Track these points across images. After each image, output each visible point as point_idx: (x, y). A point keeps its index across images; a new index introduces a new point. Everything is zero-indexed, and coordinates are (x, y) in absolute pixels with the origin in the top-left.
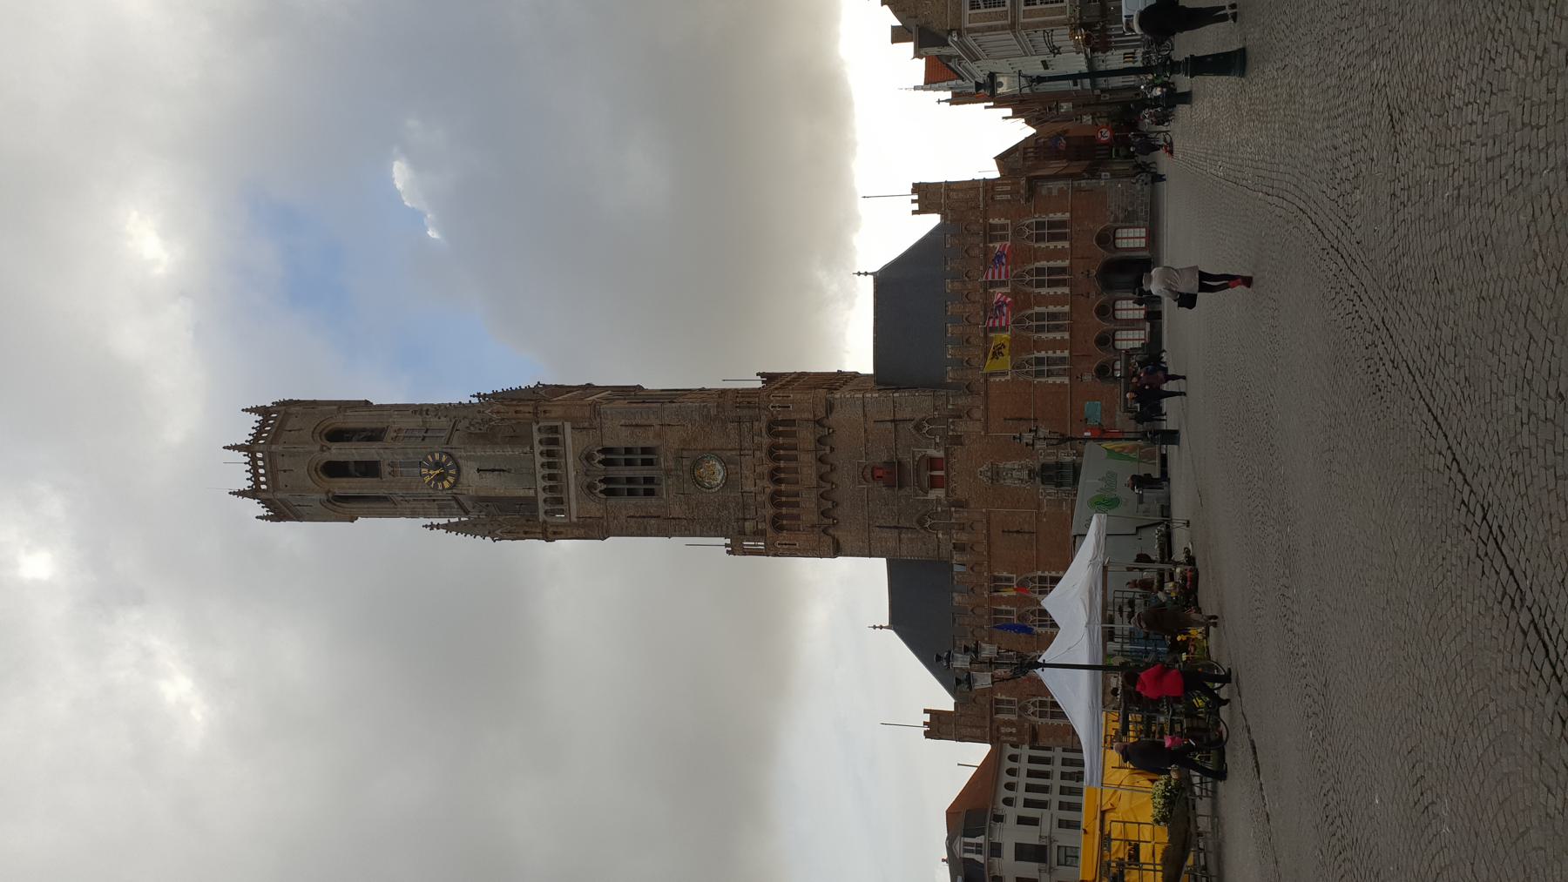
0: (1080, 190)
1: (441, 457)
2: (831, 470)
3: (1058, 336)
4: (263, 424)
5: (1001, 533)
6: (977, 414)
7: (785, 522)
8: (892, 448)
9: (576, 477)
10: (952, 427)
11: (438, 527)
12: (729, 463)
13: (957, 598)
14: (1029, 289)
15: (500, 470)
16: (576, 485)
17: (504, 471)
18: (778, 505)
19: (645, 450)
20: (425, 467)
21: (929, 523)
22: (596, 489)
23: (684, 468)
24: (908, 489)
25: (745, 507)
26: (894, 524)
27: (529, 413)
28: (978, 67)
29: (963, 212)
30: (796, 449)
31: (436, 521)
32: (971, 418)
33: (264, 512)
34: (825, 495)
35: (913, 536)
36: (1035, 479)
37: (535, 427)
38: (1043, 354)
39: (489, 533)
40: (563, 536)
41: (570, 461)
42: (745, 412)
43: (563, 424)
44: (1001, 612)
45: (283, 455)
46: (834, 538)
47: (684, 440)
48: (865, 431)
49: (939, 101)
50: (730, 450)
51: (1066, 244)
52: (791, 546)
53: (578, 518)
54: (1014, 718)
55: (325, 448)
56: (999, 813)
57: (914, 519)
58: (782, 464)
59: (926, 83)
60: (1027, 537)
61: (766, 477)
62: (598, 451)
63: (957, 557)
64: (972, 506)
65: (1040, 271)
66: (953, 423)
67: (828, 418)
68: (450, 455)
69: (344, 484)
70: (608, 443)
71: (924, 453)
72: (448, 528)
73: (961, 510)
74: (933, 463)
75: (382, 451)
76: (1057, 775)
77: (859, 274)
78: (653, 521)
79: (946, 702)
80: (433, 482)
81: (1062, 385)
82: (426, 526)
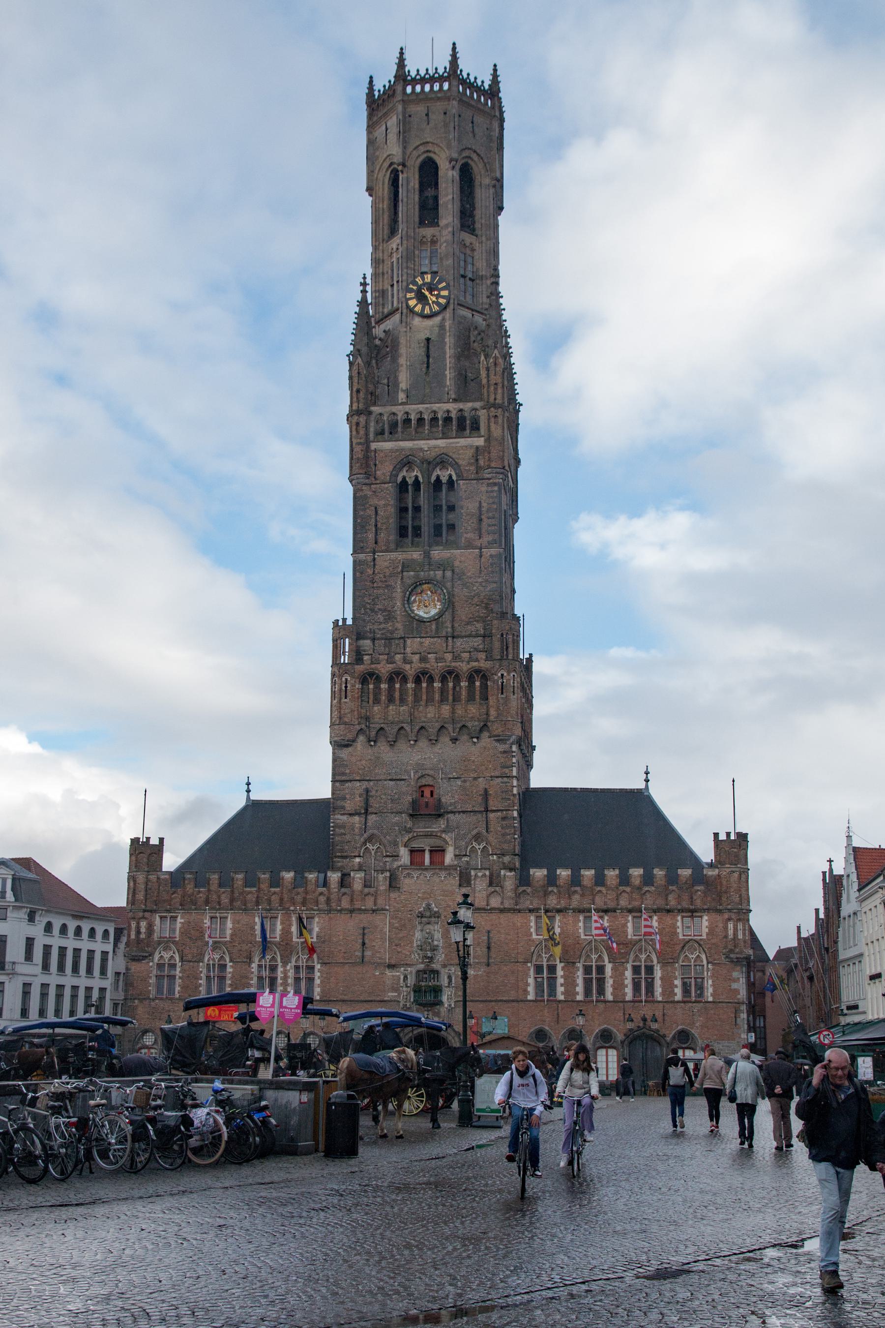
0: (737, 1012)
1: (443, 297)
2: (431, 740)
3: (580, 989)
4: (479, 89)
5: (362, 926)
6: (495, 902)
7: (371, 686)
9: (421, 449)
10: (480, 874)
11: (364, 292)
12: (437, 624)
13: (288, 876)
15: (428, 361)
16: (411, 449)
17: (428, 367)
18: (391, 680)
19: (452, 527)
20: (433, 279)
21: (371, 848)
22: (407, 471)
23: (432, 573)
27: (495, 399)
28: (871, 910)
29: (716, 888)
30: (454, 701)
31: (369, 288)
32: (490, 894)
33: (380, 85)
34: (402, 732)
35: (357, 830)
36: (422, 963)
37: (478, 405)
38: (560, 972)
39: (359, 350)
40: (354, 433)
41: (441, 443)
42: (497, 645)
43: (483, 436)
44: (274, 925)
45: (445, 113)
46: (354, 741)
47: (464, 574)
49: (830, 861)
50: (453, 627)
51: (679, 997)
52: (343, 693)
53: (375, 451)
54: (156, 936)
55: (453, 163)
56: (37, 918)
57: (375, 832)
58: (437, 685)
59: (855, 849)
60: (359, 954)
61: (423, 665)
63: (334, 877)
64: (392, 895)
65: (650, 969)
66: (484, 875)
67: (490, 737)
68: (445, 308)
69: (412, 184)
72: (363, 303)
74: (438, 852)
75: (450, 229)
76: (75, 981)
77: (647, 773)
78: (371, 536)
79: (171, 861)
80: (415, 288)
81: (526, 992)
82: (364, 278)
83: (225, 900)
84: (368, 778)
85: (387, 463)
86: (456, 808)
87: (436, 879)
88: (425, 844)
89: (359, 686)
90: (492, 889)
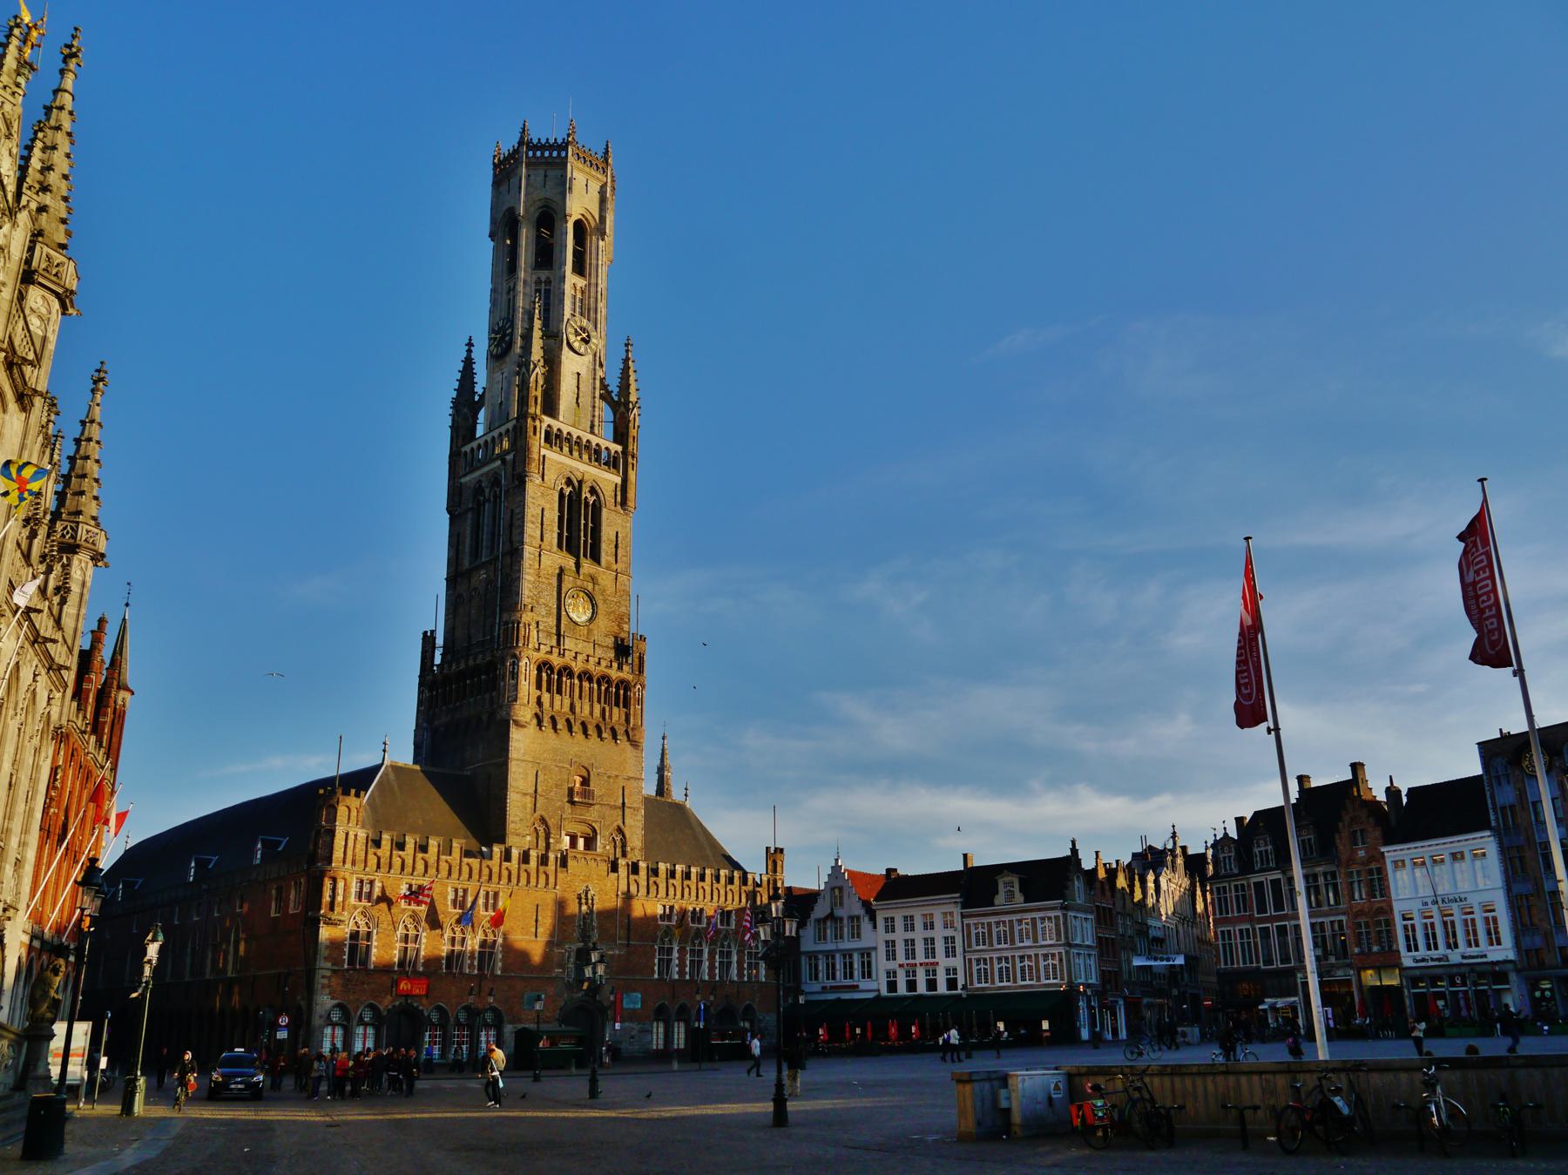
1: (594, 344)
3: (687, 969)
8: (602, 800)
14: (719, 944)
15: (578, 394)
16: (571, 467)
18: (560, 674)
24: (570, 811)
25: (549, 634)
26: (539, 790)
37: (619, 448)
48: (617, 776)
57: (544, 813)
62: (595, 500)
70: (604, 511)
71: (598, 832)
73: (559, 863)
77: (686, 789)
78: (539, 532)
83: (420, 866)
84: (538, 761)
85: (553, 471)
86: (602, 800)
87: (592, 864)
88: (579, 829)
89: (536, 672)
90: (632, 877)
